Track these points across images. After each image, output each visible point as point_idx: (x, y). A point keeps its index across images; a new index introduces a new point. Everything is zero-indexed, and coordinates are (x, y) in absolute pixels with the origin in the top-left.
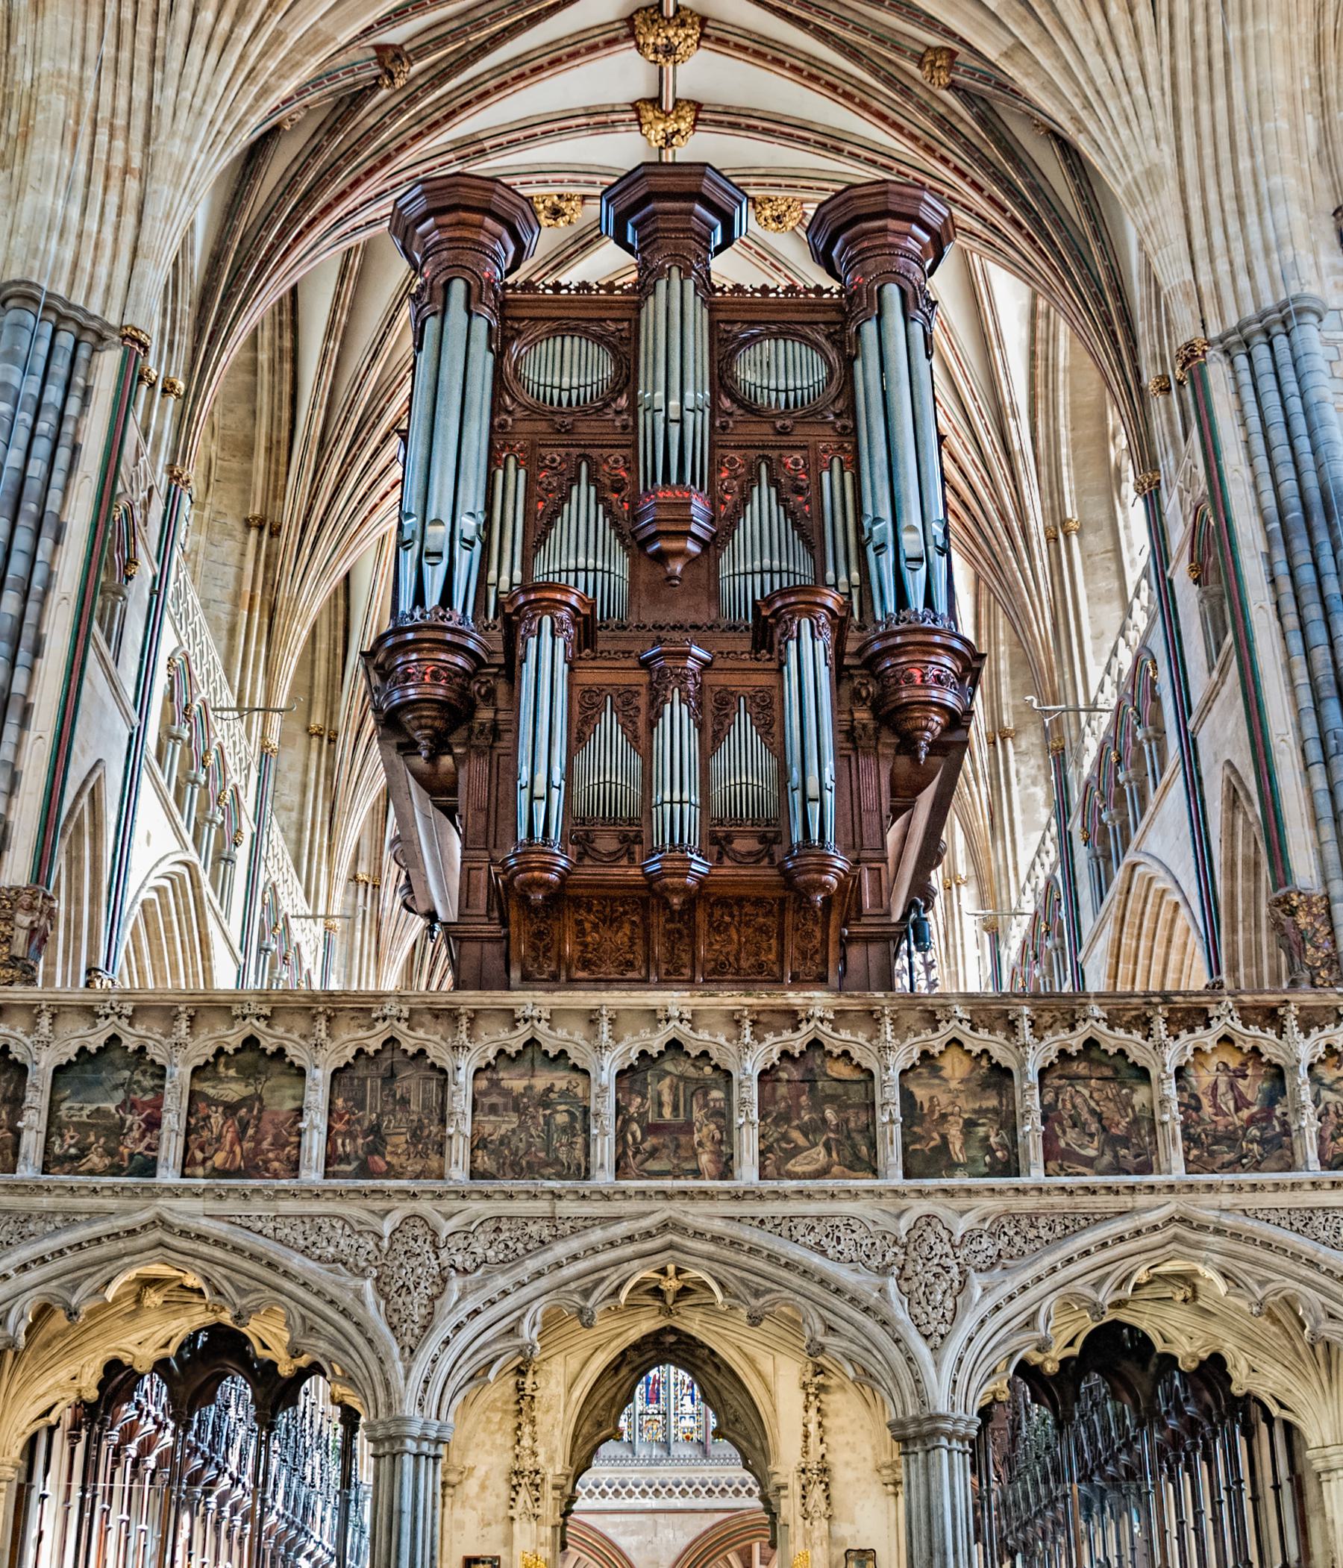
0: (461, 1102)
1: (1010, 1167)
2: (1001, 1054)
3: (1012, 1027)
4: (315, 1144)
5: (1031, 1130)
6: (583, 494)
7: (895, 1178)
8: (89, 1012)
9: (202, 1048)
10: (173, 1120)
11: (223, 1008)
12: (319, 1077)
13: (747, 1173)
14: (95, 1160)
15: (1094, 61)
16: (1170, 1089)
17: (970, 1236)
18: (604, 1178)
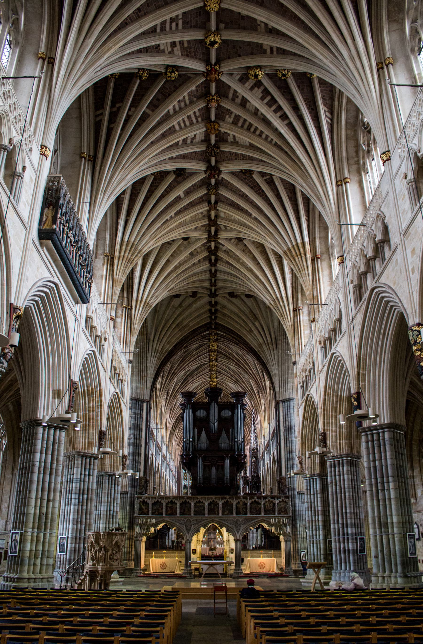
0: (192, 507)
1: (246, 514)
2: (246, 502)
3: (247, 499)
4: (178, 511)
5: (248, 510)
6: (203, 432)
7: (235, 515)
8: (155, 498)
9: (167, 501)
10: (164, 510)
11: (169, 497)
12: (178, 504)
13: (220, 515)
14: (157, 513)
15: (269, 357)
16: (263, 506)
17: (242, 521)
18: (206, 515)
